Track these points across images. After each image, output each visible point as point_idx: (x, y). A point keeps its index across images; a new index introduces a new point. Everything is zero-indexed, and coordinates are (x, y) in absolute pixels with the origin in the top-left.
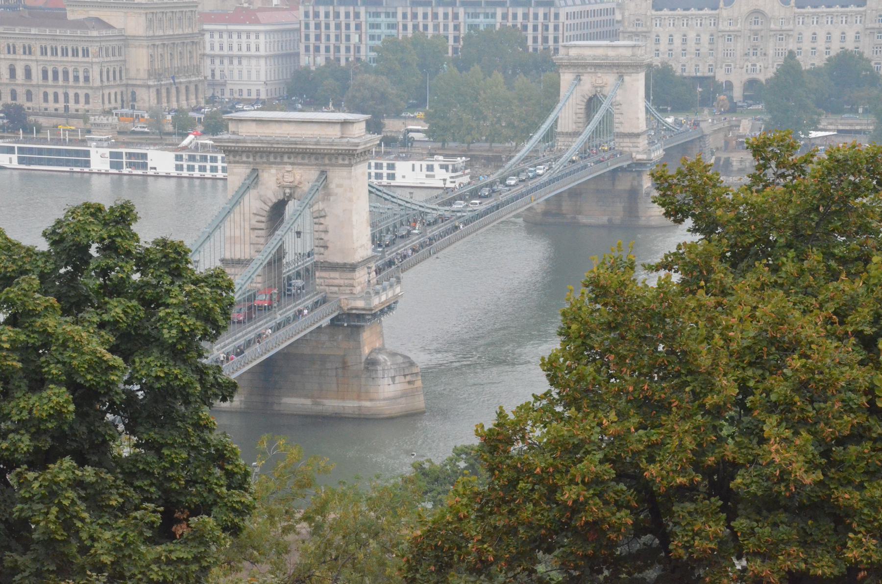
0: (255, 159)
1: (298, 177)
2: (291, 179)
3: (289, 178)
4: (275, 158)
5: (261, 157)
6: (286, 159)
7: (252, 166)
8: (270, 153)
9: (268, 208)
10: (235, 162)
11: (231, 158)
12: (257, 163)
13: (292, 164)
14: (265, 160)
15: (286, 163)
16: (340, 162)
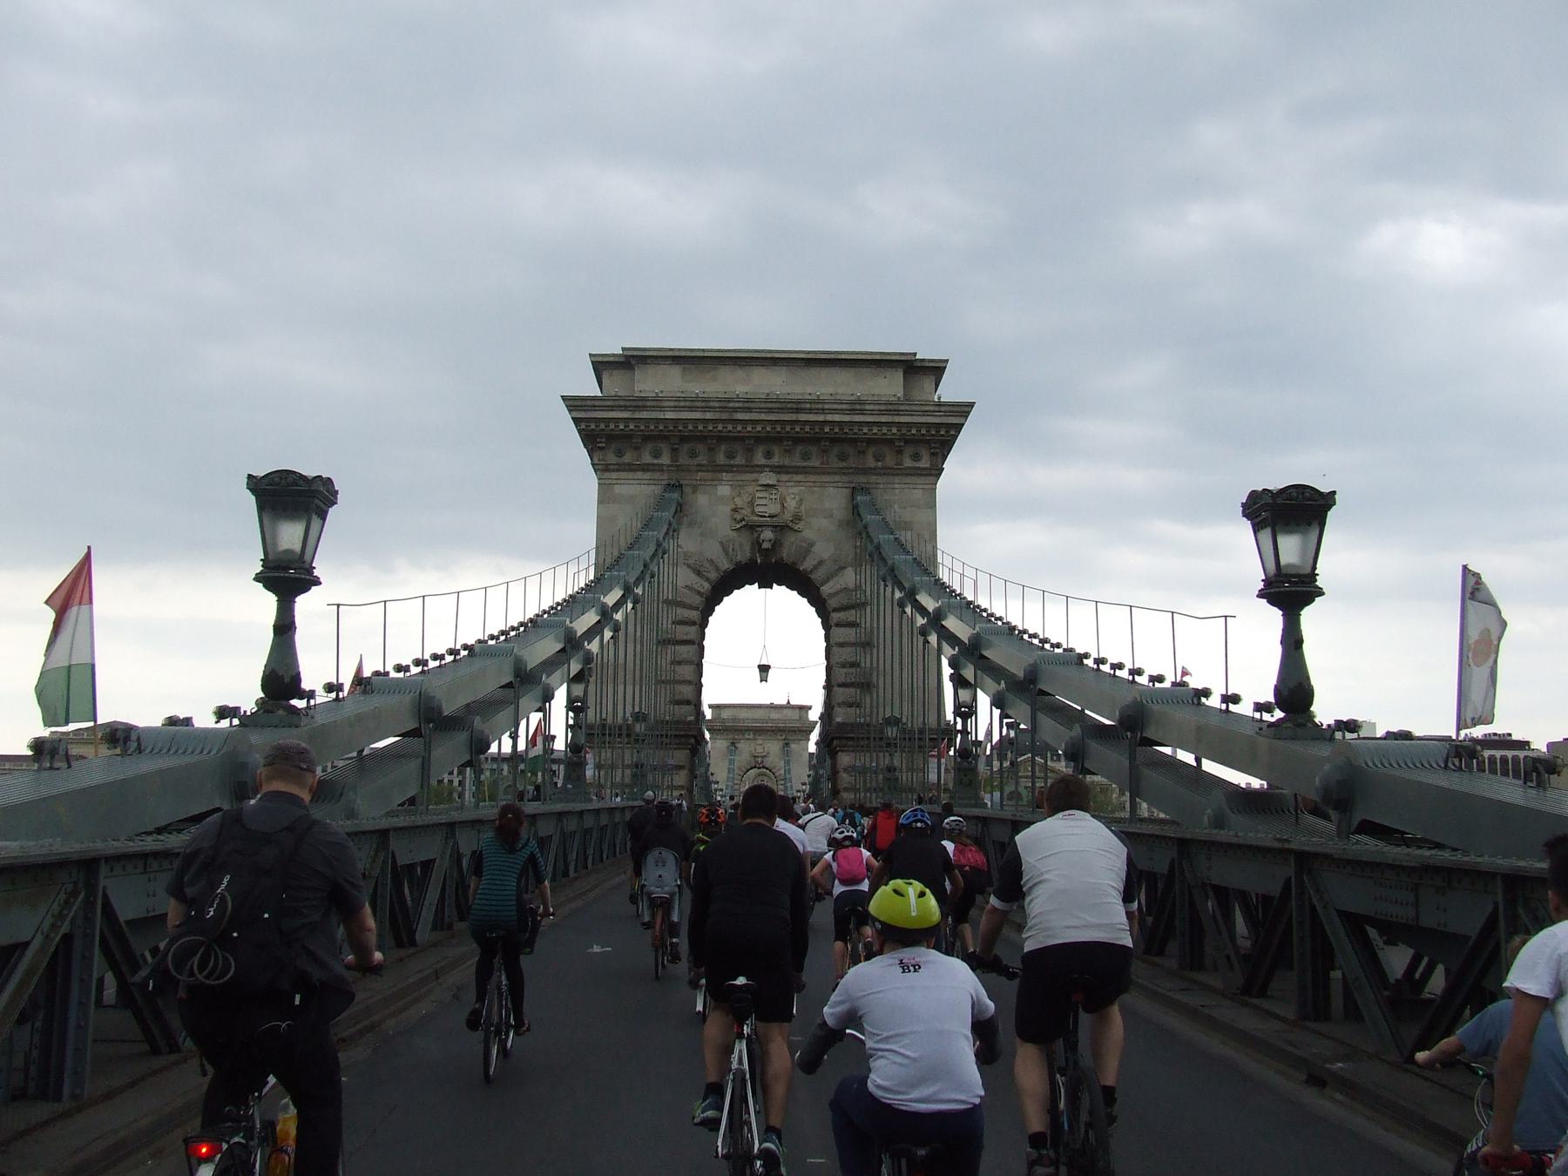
0: (674, 459)
1: (791, 504)
2: (774, 508)
3: (767, 506)
4: (731, 456)
5: (693, 454)
6: (759, 459)
7: (664, 478)
8: (721, 439)
9: (707, 586)
10: (621, 468)
11: (612, 459)
12: (680, 469)
13: (779, 470)
14: (702, 459)
15: (760, 469)
16: (908, 463)
